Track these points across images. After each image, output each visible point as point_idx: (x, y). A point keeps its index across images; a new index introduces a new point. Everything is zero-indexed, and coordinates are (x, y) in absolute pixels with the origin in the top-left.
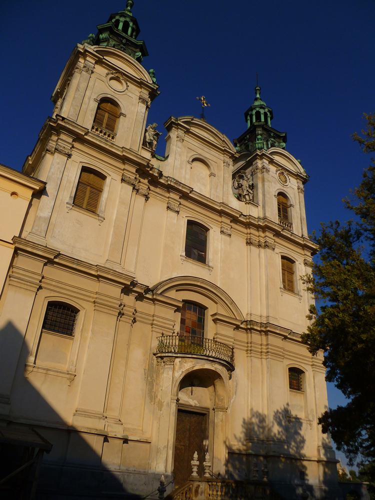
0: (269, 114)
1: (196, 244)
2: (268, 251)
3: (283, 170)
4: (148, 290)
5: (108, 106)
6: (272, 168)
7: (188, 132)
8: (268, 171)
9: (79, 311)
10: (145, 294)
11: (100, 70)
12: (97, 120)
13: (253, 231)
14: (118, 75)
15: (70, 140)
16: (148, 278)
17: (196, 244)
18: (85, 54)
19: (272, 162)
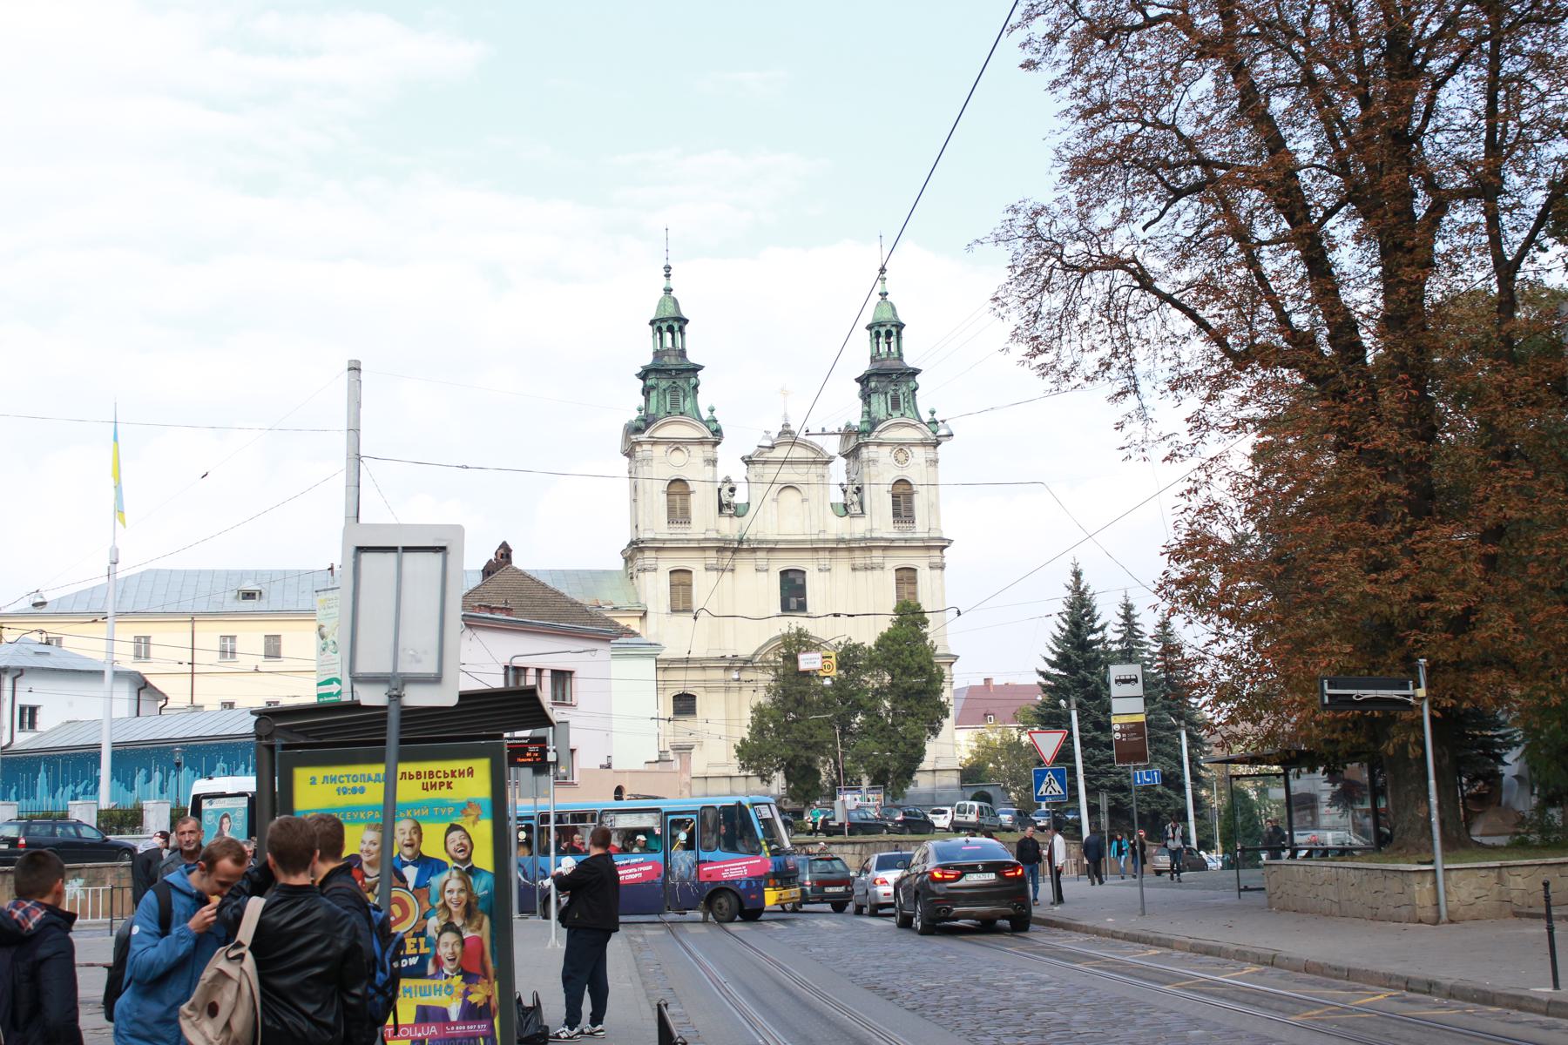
0: (894, 330)
1: (793, 591)
2: (877, 573)
3: (901, 446)
4: (746, 661)
5: (676, 488)
6: (886, 450)
7: (765, 462)
8: (874, 461)
9: (693, 697)
10: (746, 664)
11: (660, 450)
12: (672, 518)
13: (857, 554)
14: (677, 444)
15: (653, 554)
16: (745, 651)
17: (793, 591)
18: (639, 443)
19: (880, 444)
